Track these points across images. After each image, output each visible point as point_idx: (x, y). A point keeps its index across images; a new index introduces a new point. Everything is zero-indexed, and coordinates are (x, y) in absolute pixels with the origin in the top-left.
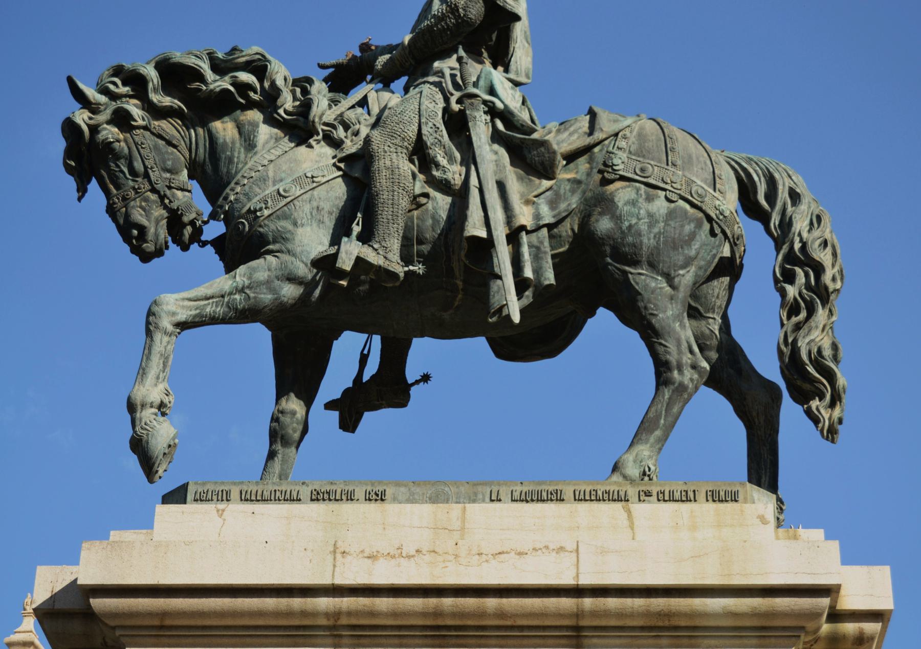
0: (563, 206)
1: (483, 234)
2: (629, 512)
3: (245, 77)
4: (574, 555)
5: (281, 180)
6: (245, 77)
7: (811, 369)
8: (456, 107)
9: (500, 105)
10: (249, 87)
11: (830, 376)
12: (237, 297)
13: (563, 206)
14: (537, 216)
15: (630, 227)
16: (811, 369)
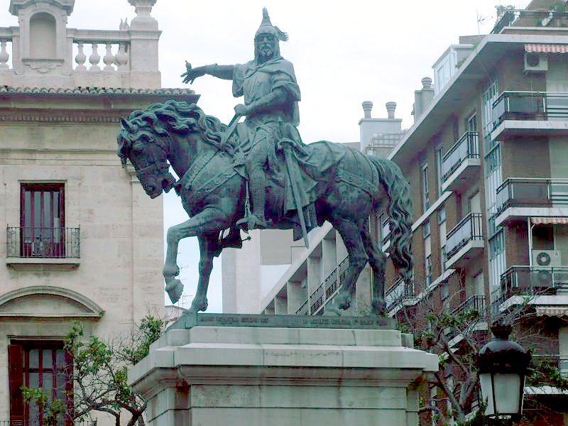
0: (320, 192)
1: (293, 208)
2: (353, 331)
3: (192, 120)
4: (341, 356)
5: (214, 176)
6: (192, 120)
7: (403, 258)
8: (280, 147)
9: (295, 144)
10: (194, 125)
11: (409, 259)
12: (201, 228)
13: (320, 192)
14: (311, 198)
15: (345, 202)
16: (403, 258)
